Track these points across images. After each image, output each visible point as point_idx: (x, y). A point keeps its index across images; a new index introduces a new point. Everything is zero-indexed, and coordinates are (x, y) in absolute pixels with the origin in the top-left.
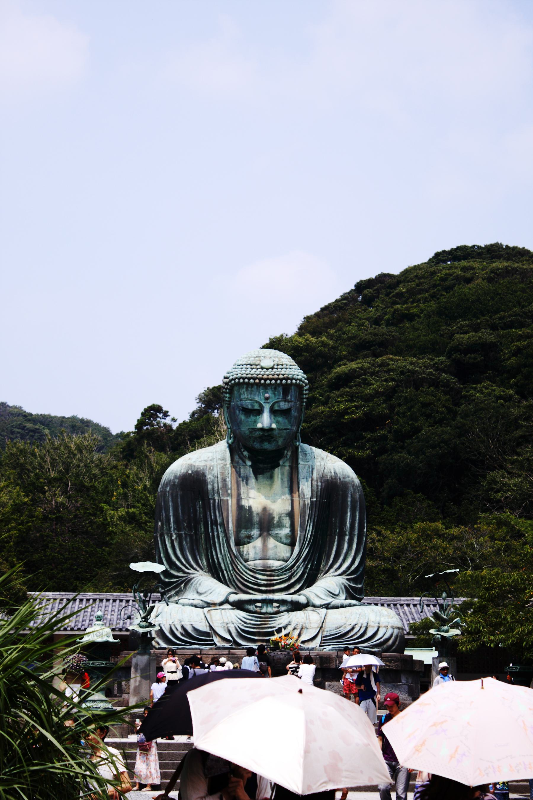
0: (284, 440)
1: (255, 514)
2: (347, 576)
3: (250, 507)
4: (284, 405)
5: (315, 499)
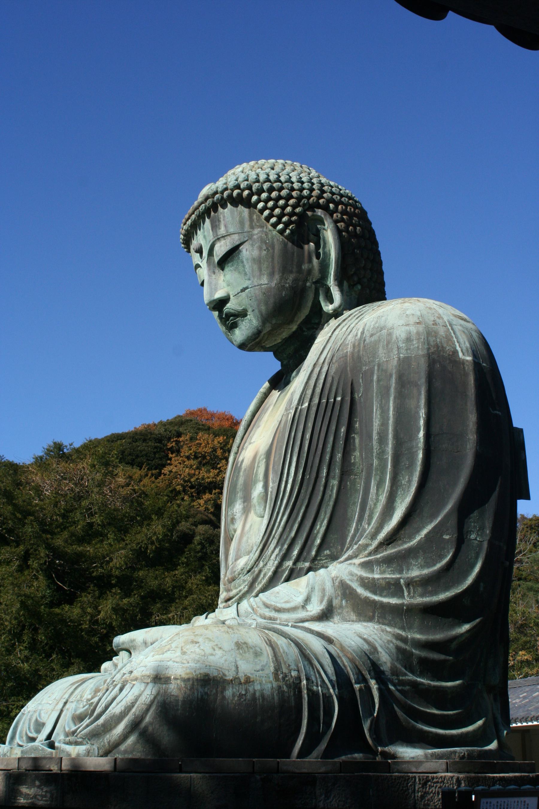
0: (253, 311)
1: (241, 473)
2: (370, 554)
3: (243, 461)
4: (221, 249)
5: (306, 405)
